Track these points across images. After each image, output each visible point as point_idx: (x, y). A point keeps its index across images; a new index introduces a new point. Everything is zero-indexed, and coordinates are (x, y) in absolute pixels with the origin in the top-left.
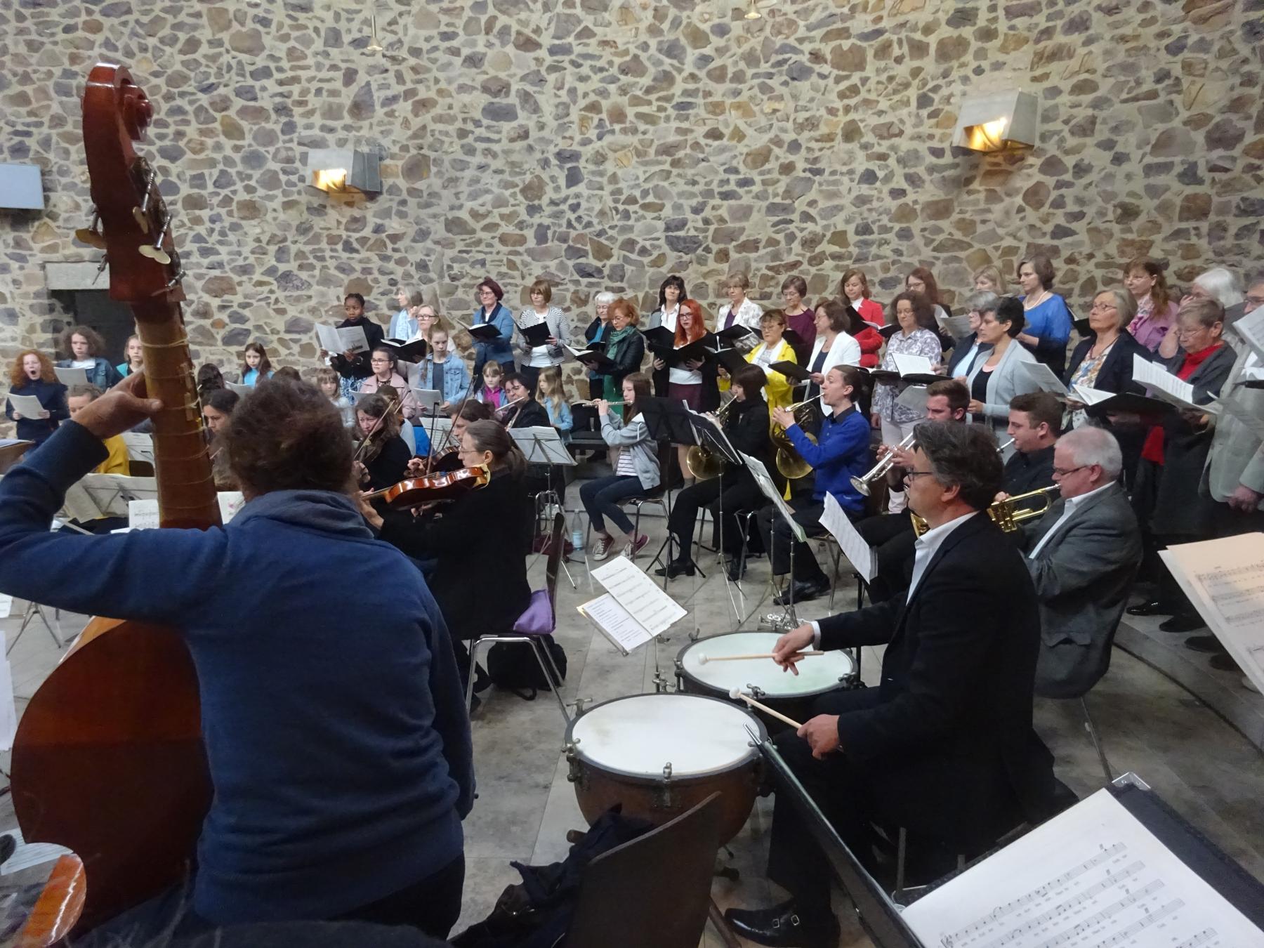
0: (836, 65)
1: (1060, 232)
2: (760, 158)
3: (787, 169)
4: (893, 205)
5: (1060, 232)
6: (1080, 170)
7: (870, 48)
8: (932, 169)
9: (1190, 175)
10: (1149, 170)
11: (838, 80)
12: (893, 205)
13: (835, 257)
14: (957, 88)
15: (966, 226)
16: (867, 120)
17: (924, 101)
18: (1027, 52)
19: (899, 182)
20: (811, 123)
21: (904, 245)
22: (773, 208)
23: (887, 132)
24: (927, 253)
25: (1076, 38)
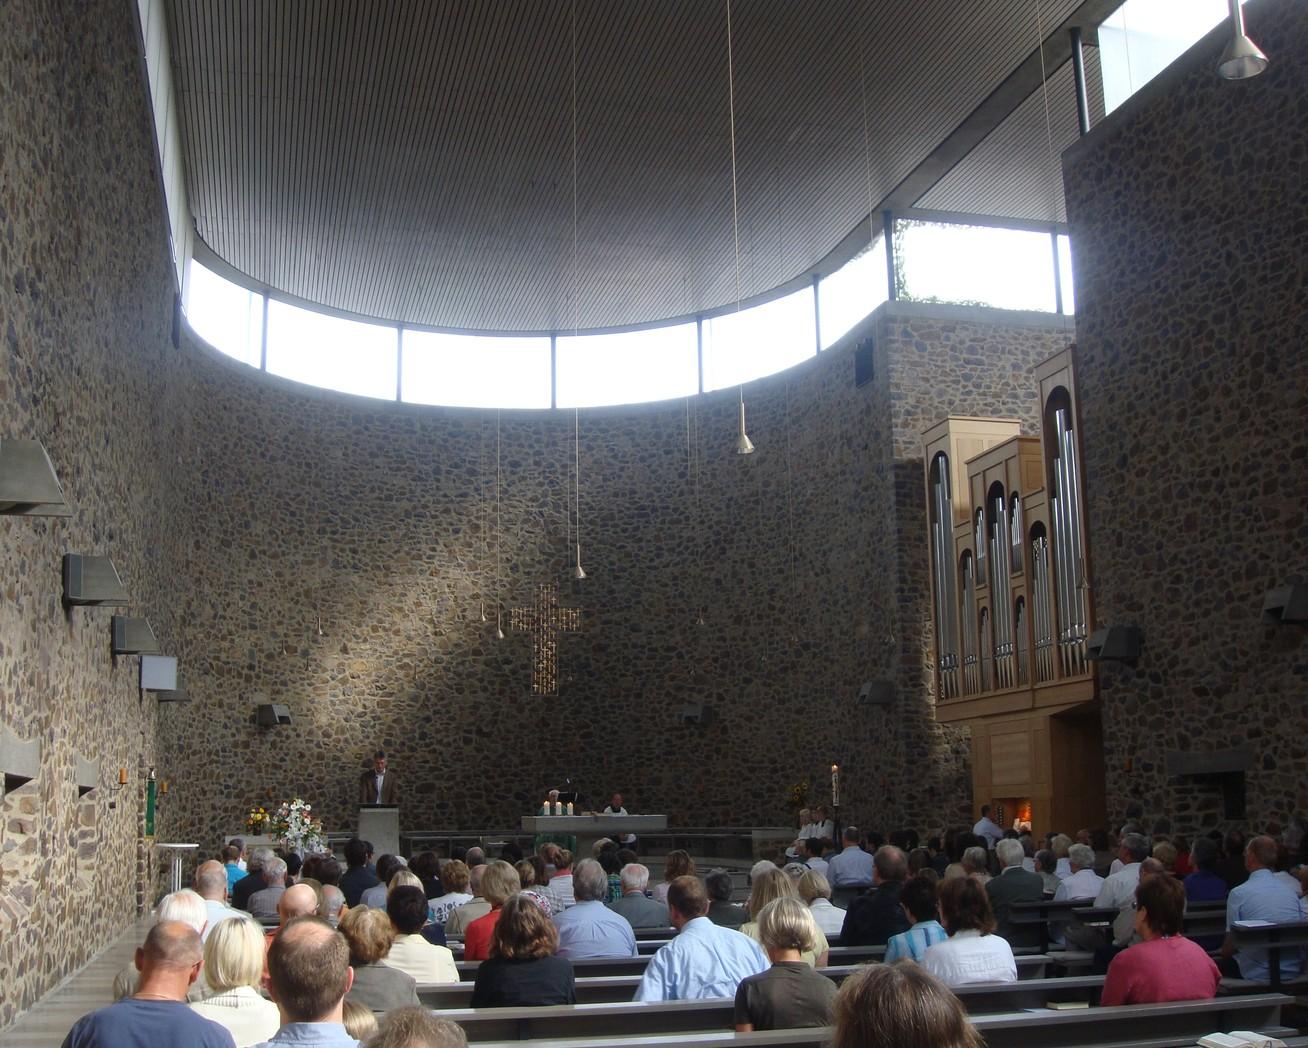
0: (218, 673)
1: (282, 760)
2: (198, 708)
3: (204, 716)
4: (232, 740)
5: (282, 760)
6: (288, 737)
7: (227, 667)
8: (244, 727)
9: (318, 746)
10: (307, 741)
11: (218, 679)
12: (232, 740)
13: (217, 762)
14: (249, 695)
15: (254, 753)
16: (226, 701)
17: (241, 698)
18: (268, 689)
19: (234, 731)
20: (209, 697)
21: (235, 759)
22: (201, 735)
23: (231, 707)
24: (243, 764)
25: (284, 688)
